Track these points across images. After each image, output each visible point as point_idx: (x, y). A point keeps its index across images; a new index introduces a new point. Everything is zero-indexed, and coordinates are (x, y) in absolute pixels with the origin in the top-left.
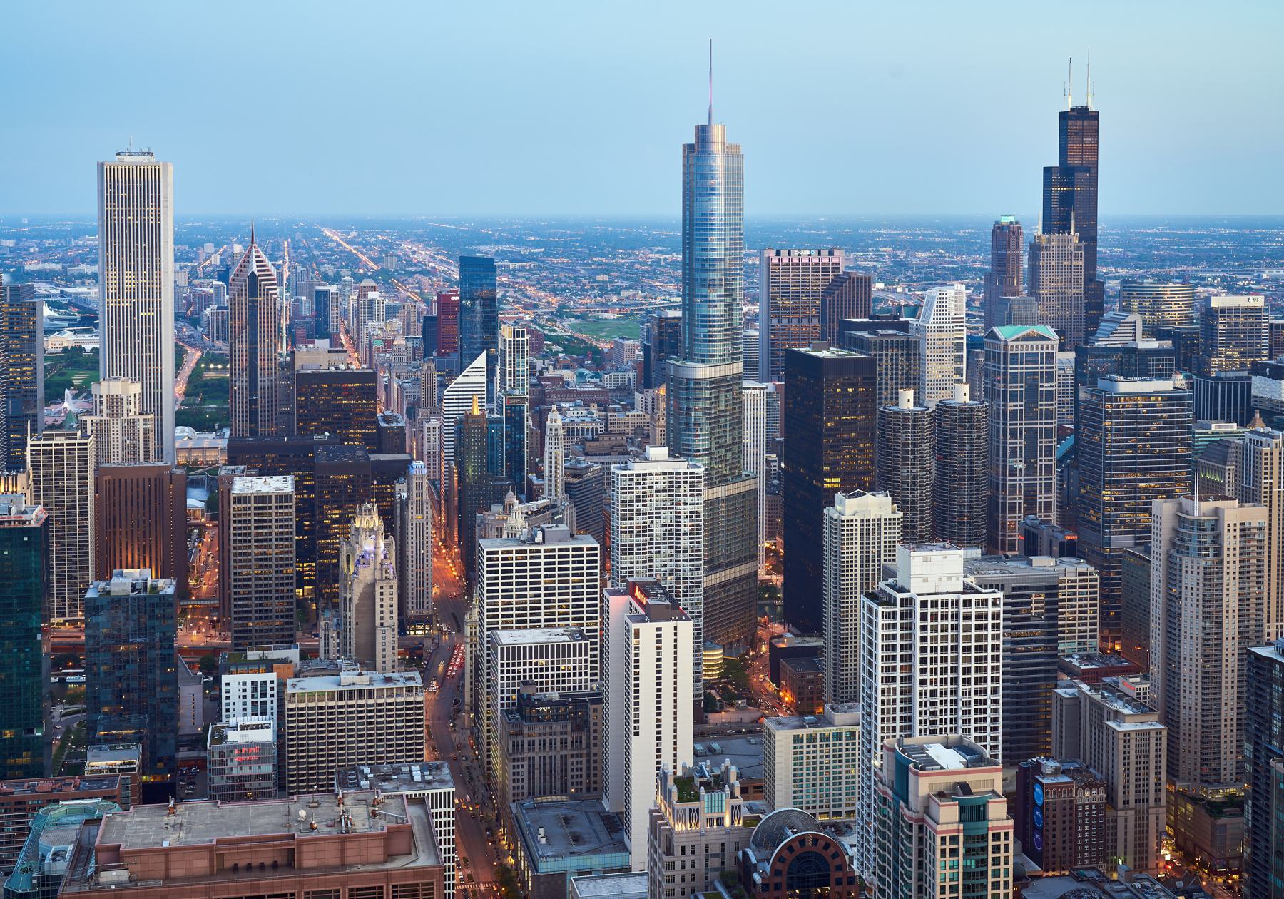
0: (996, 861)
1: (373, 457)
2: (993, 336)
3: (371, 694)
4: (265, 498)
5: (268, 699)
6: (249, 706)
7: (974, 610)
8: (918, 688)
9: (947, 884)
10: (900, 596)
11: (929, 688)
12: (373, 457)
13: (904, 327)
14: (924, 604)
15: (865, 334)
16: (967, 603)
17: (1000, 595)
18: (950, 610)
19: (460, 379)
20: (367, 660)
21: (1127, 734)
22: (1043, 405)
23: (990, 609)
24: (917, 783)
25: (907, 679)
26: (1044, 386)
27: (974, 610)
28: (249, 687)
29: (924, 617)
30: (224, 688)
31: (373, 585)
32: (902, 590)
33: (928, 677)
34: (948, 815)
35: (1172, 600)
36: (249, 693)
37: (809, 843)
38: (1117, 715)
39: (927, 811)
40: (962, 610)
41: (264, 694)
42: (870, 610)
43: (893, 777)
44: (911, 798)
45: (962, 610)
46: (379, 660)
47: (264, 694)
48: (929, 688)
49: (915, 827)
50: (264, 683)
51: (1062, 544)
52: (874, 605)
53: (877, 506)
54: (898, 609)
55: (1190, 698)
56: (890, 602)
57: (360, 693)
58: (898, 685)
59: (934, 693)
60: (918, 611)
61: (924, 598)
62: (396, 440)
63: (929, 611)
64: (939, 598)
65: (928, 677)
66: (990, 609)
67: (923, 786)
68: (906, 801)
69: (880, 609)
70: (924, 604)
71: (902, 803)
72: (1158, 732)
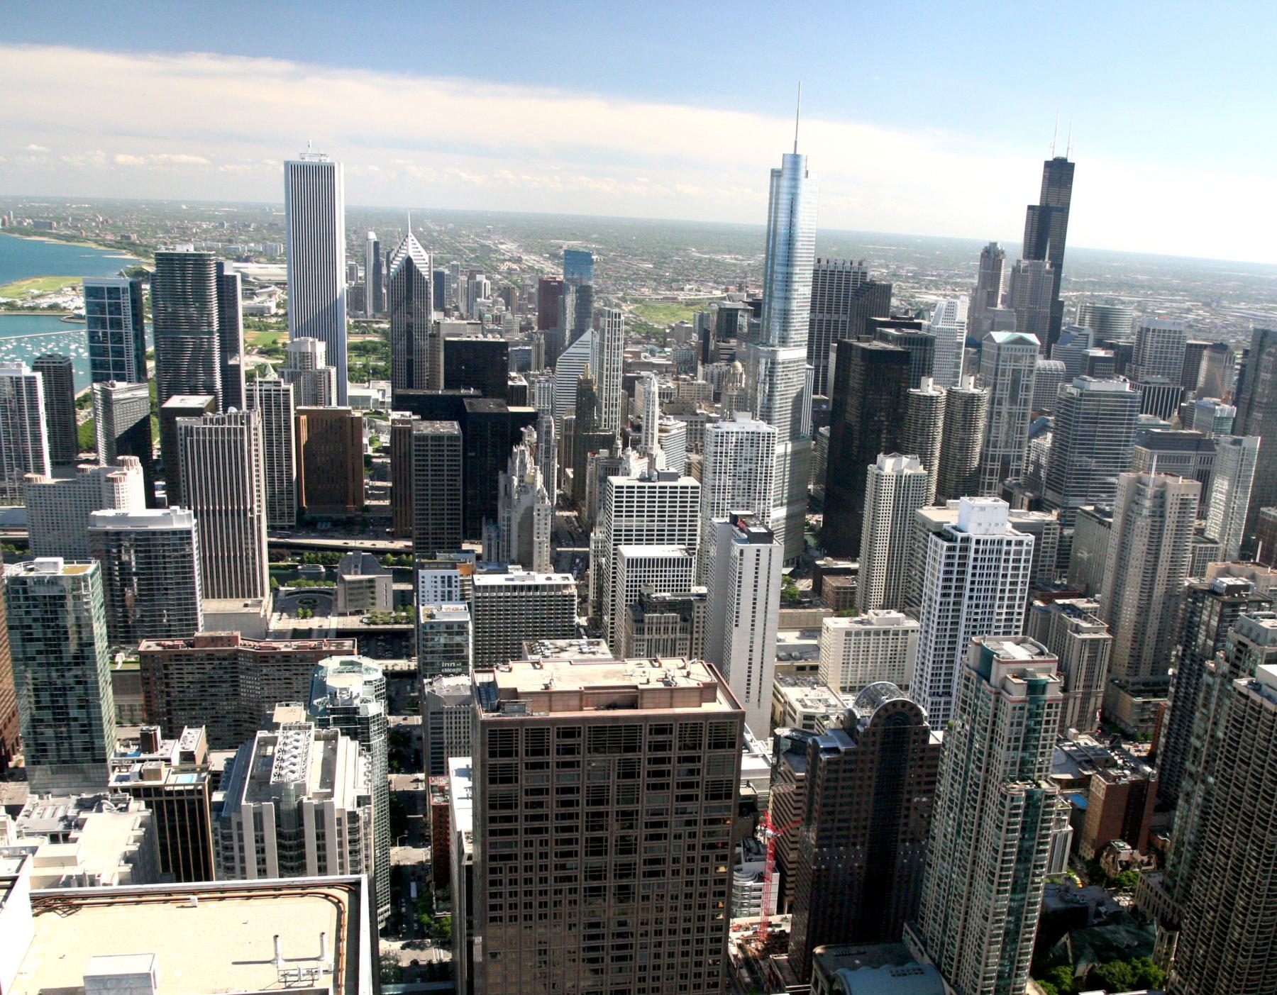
0: (1048, 722)
1: (512, 409)
2: (991, 339)
3: (537, 588)
4: (438, 438)
5: (453, 589)
6: (439, 594)
7: (1013, 548)
8: (966, 601)
9: (1013, 737)
10: (960, 535)
11: (974, 602)
12: (512, 409)
13: (919, 326)
14: (978, 542)
15: (892, 331)
16: (1009, 543)
17: (1032, 537)
18: (996, 547)
19: (571, 350)
20: (527, 564)
21: (1084, 641)
22: (1022, 395)
23: (1025, 548)
24: (998, 669)
25: (958, 595)
26: (1023, 381)
27: (1013, 548)
28: (439, 580)
29: (977, 551)
30: (421, 579)
31: (531, 509)
32: (961, 531)
33: (975, 594)
34: (1017, 691)
35: (1124, 546)
36: (439, 584)
37: (899, 706)
38: (1078, 630)
39: (1004, 688)
40: (1005, 548)
41: (450, 586)
42: (936, 545)
43: (978, 662)
44: (993, 679)
45: (1005, 548)
46: (536, 563)
47: (450, 586)
48: (974, 602)
49: (993, 697)
50: (450, 577)
51: (1030, 501)
52: (940, 541)
53: (908, 465)
54: (958, 545)
55: (1128, 614)
56: (951, 539)
57: (529, 588)
58: (952, 599)
59: (977, 606)
60: (973, 546)
61: (979, 537)
62: (519, 396)
63: (981, 547)
64: (989, 538)
65: (975, 594)
66: (1025, 548)
67: (998, 672)
68: (988, 680)
69: (946, 544)
70: (978, 542)
71: (984, 682)
72: (1105, 640)
